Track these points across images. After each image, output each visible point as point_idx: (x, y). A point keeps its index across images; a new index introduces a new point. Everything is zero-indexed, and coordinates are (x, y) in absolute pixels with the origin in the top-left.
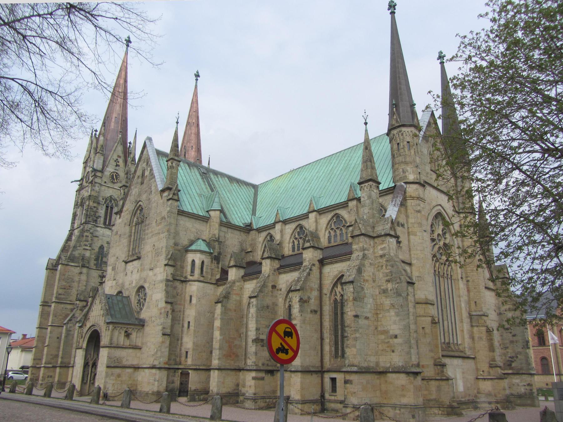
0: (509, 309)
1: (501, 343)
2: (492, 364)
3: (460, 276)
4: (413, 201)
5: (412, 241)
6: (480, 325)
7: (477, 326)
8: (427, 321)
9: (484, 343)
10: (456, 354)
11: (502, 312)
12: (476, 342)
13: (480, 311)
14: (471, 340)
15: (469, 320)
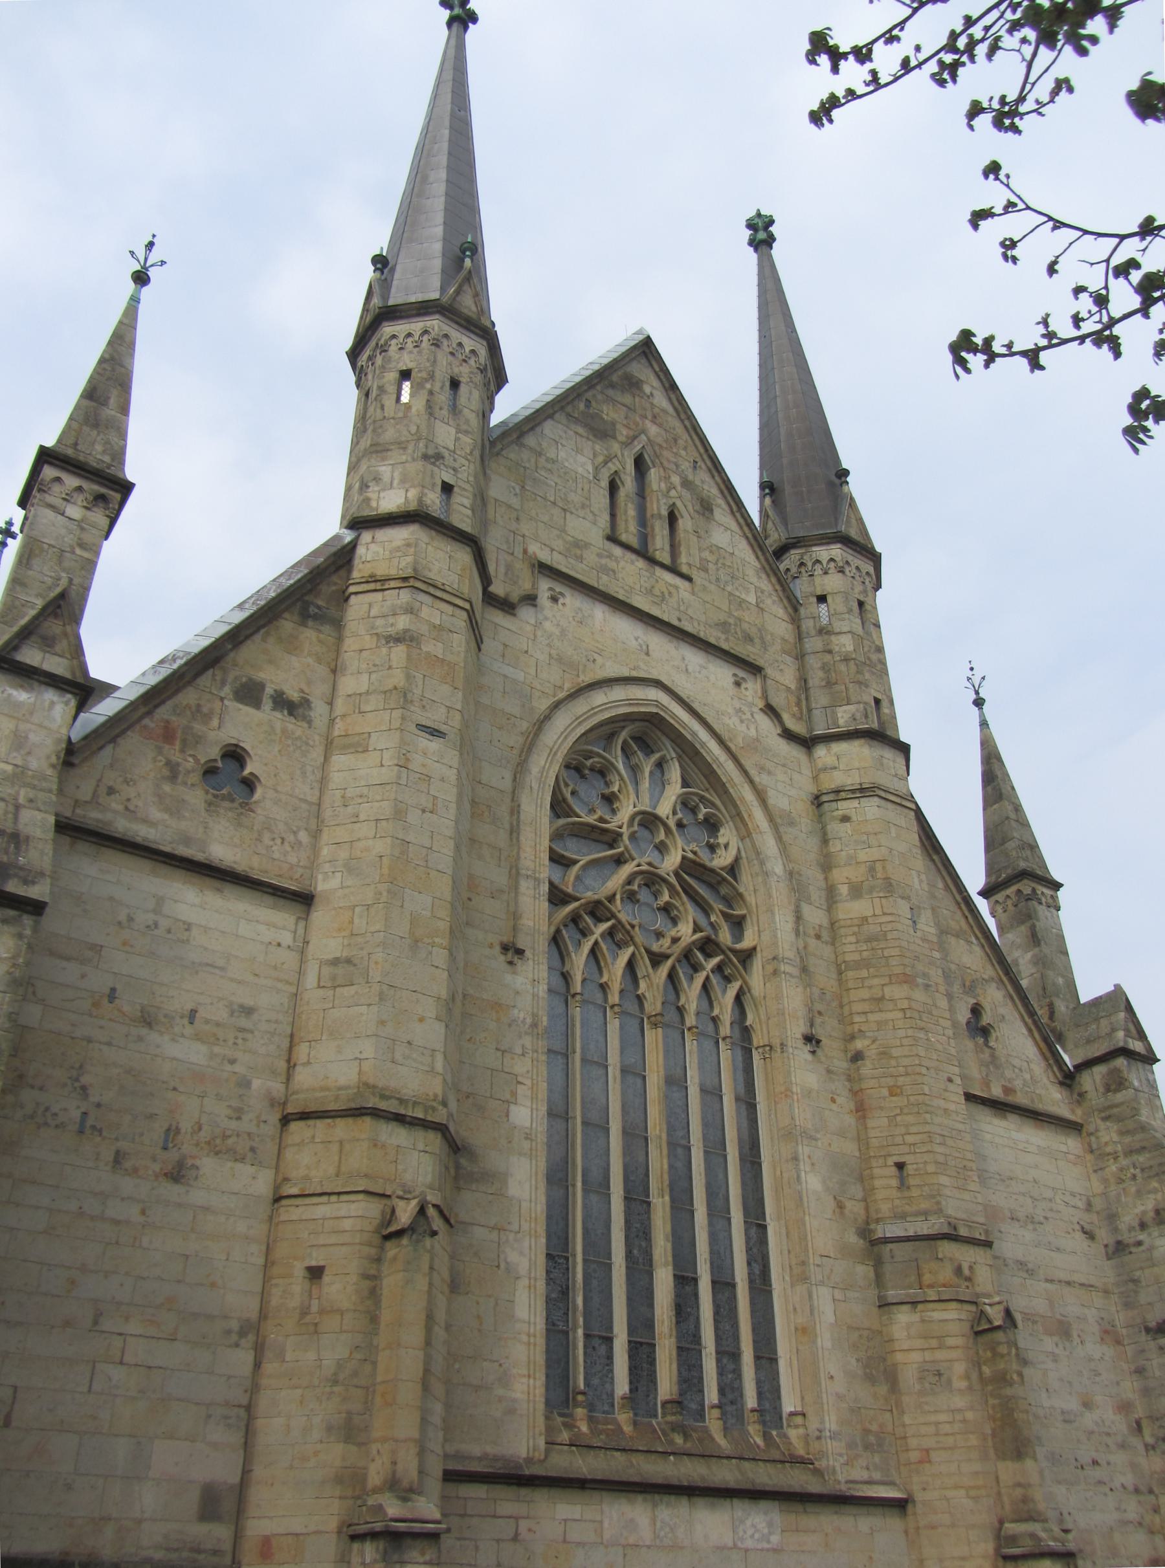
0: (1157, 1212)
1: (1140, 1412)
2: (1013, 1540)
3: (797, 1029)
4: (379, 595)
5: (337, 779)
6: (932, 1295)
7: (914, 1304)
8: (347, 1224)
9: (959, 1402)
10: (724, 1474)
11: (1127, 1238)
12: (906, 1399)
13: (925, 1214)
14: (883, 1389)
15: (863, 1271)
